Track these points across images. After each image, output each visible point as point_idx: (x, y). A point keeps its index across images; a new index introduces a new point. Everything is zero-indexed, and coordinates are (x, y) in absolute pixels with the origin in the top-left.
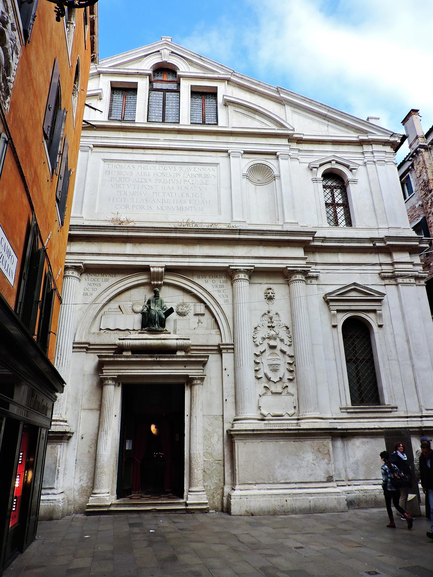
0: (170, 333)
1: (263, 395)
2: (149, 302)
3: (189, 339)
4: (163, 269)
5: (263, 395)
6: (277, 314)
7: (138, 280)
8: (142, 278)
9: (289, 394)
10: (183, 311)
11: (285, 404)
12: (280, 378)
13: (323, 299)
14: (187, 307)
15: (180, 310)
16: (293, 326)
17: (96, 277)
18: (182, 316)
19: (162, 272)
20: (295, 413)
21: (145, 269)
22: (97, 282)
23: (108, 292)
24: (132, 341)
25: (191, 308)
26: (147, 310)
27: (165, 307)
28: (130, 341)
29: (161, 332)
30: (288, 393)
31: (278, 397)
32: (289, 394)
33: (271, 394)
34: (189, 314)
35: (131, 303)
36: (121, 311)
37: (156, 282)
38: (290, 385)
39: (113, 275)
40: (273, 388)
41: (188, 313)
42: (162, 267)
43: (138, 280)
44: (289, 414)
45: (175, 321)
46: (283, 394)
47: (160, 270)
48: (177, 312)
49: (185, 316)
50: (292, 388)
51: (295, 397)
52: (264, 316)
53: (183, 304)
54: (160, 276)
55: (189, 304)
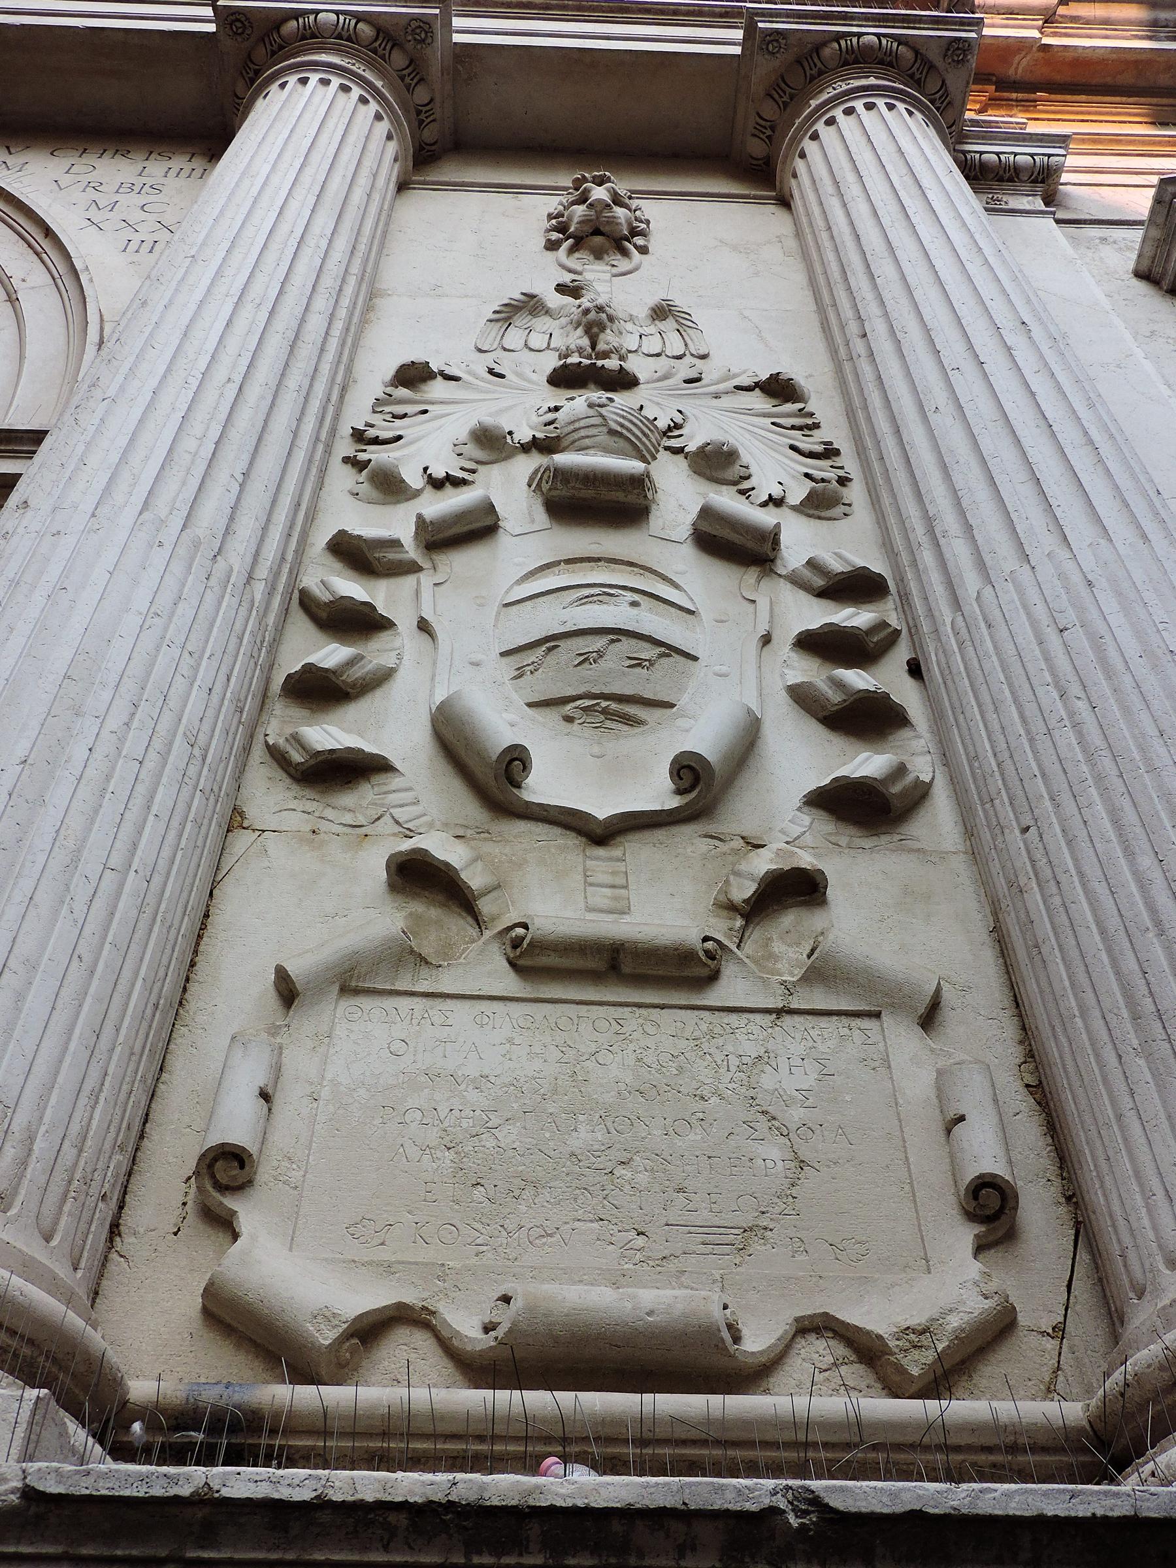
1: (352, 981)
5: (352, 981)
6: (661, 312)
9: (851, 993)
11: (773, 1152)
12: (689, 771)
13: (1141, 287)
16: (841, 362)
20: (998, 1329)
30: (821, 971)
31: (622, 1044)
32: (851, 993)
33: (509, 983)
38: (859, 874)
40: (556, 896)
44: (866, 1350)
46: (733, 987)
50: (875, 907)
51: (980, 1032)
52: (521, 320)
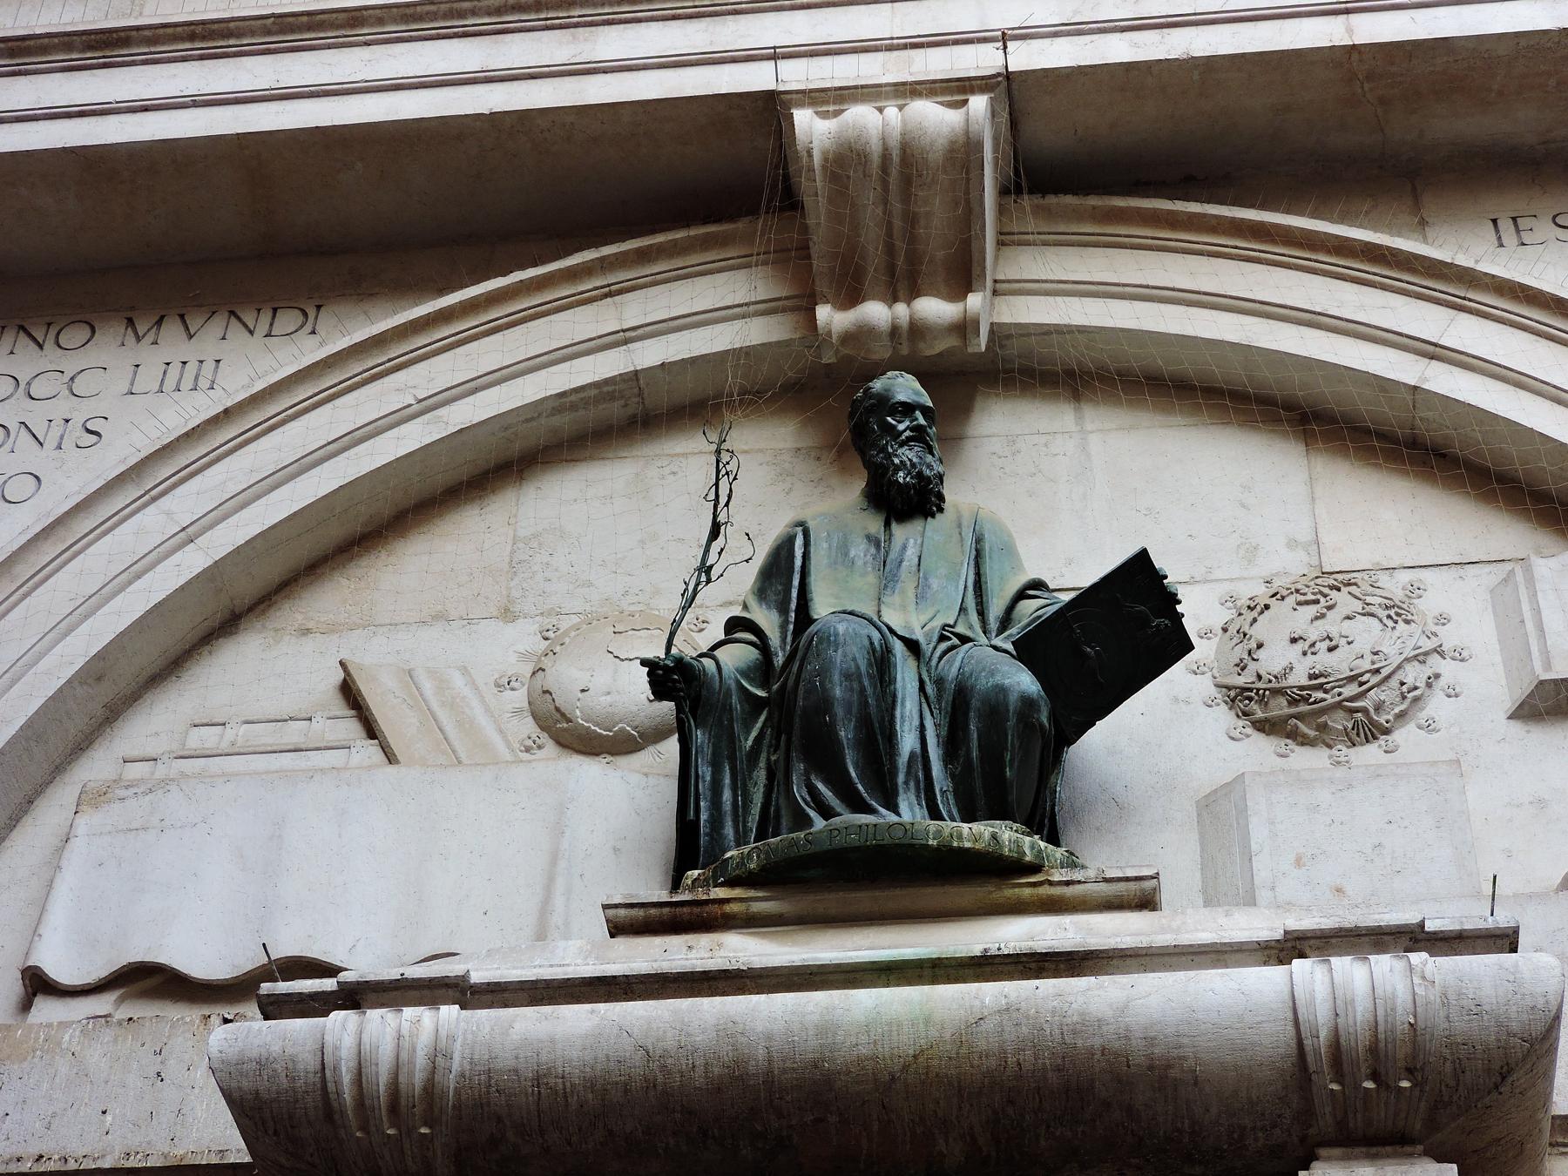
0: (1147, 902)
2: (782, 573)
3: (1507, 940)
4: (979, 104)
7: (624, 338)
8: (702, 311)
10: (1338, 663)
14: (1396, 613)
15: (1278, 658)
17: (51, 357)
18: (1322, 737)
19: (964, 152)
21: (716, 178)
22: (63, 407)
23: (188, 502)
24: (485, 1018)
25: (1449, 637)
26: (763, 669)
27: (1028, 607)
28: (449, 1012)
29: (988, 880)
34: (1437, 706)
35: (523, 638)
36: (371, 731)
37: (875, 312)
39: (288, 320)
41: (1413, 699)
42: (957, 89)
43: (624, 338)
45: (1220, 811)
47: (935, 119)
48: (1240, 698)
49: (1369, 730)
53: (1324, 589)
54: (936, 212)
55: (1415, 590)
